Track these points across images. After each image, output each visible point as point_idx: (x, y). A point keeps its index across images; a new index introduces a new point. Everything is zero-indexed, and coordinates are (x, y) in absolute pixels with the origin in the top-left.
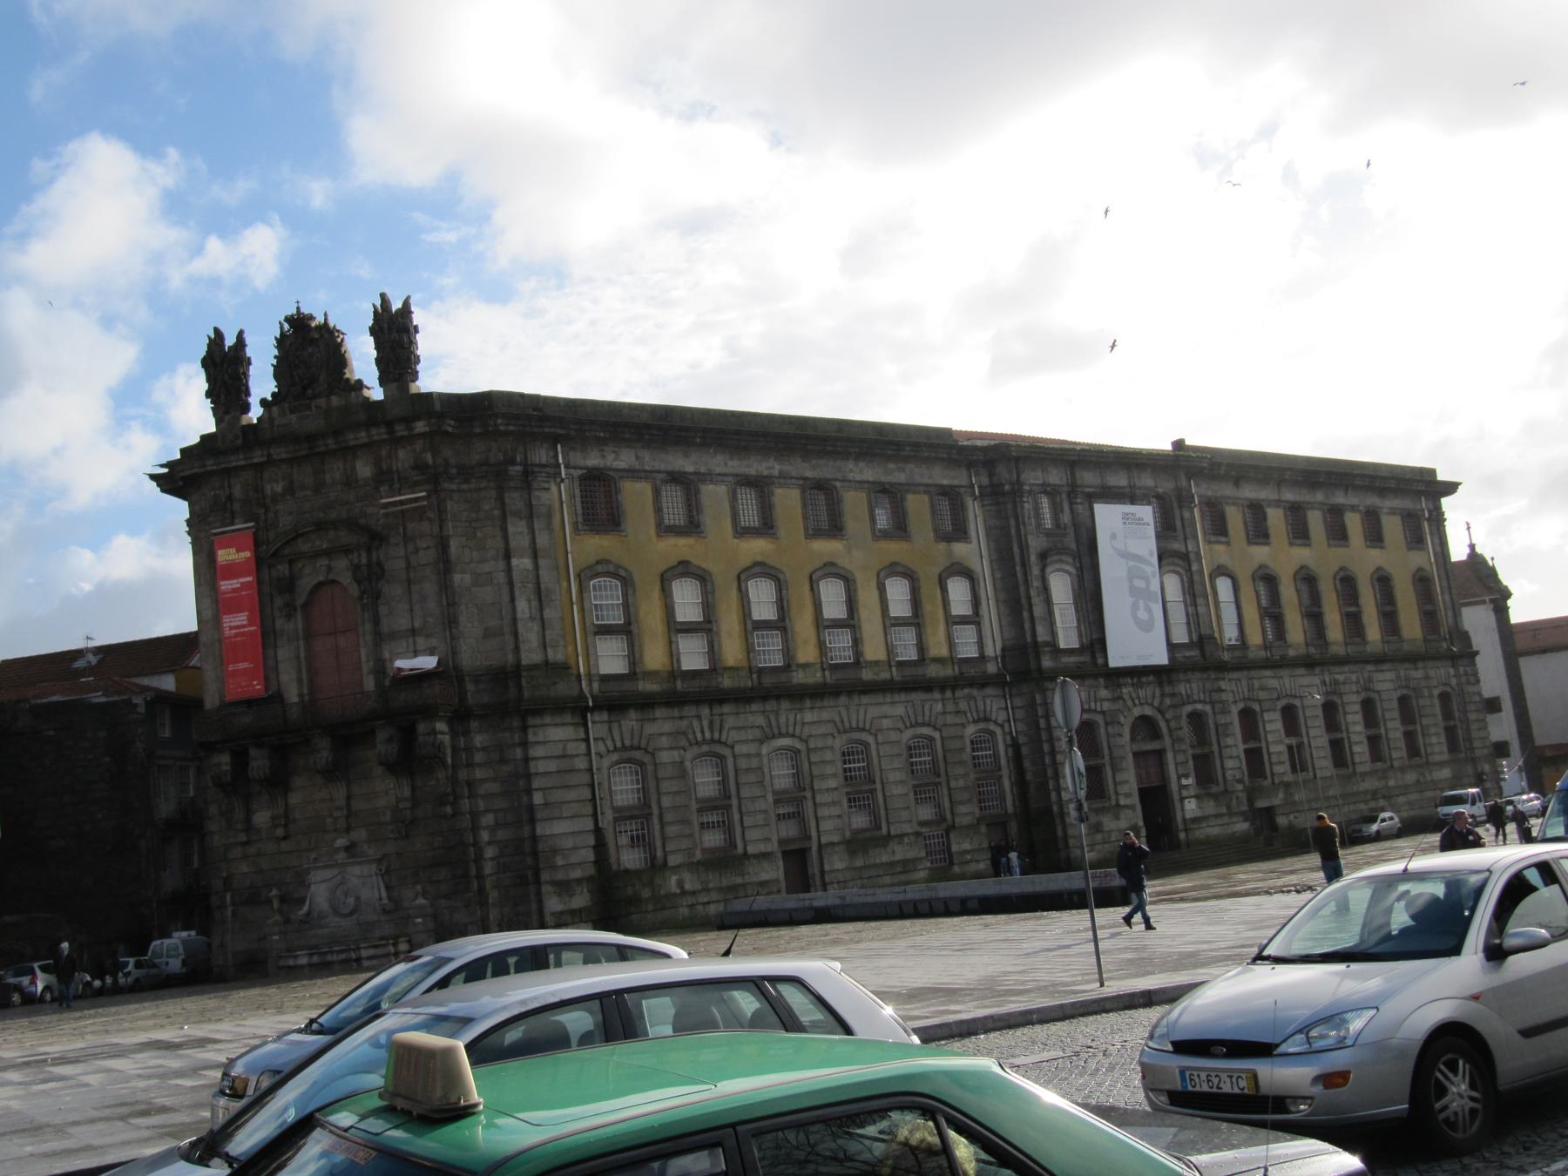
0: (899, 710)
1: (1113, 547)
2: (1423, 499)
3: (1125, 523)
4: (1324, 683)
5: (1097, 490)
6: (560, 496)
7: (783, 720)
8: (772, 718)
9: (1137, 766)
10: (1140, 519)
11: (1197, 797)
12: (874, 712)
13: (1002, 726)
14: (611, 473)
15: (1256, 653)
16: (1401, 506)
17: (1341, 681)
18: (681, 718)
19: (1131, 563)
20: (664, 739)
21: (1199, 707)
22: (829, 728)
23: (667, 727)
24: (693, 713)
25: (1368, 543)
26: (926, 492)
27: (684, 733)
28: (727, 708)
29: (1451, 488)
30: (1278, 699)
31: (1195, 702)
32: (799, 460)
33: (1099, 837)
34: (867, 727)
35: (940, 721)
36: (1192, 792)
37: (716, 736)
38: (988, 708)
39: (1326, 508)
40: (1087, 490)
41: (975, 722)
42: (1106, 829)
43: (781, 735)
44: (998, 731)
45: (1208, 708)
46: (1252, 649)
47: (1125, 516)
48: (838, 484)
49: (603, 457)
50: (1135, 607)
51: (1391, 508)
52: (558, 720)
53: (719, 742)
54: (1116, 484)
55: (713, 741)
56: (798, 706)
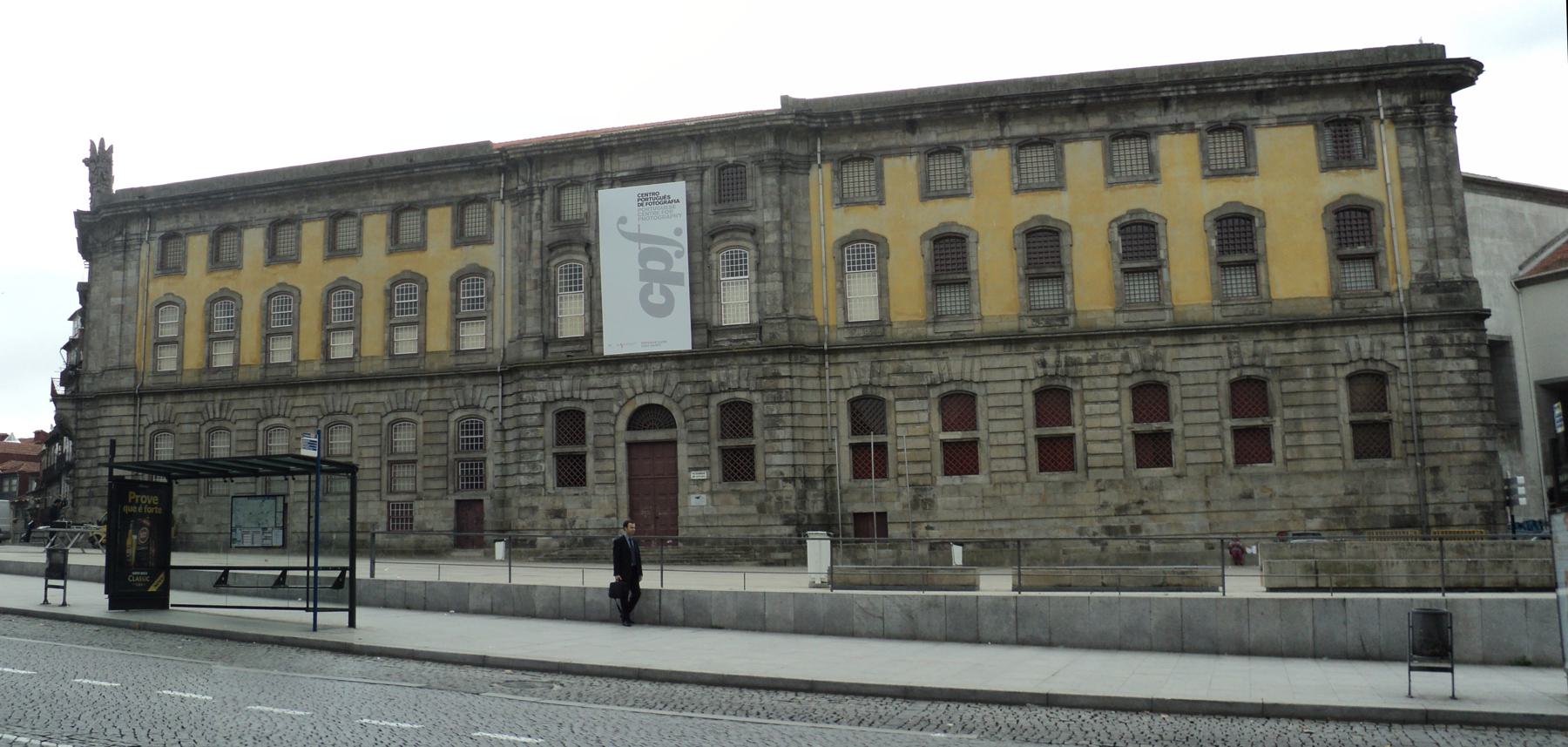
0: (383, 397)
1: (623, 234)
2: (1379, 94)
3: (642, 205)
4: (1044, 364)
5: (635, 173)
6: (148, 253)
7: (276, 403)
8: (269, 402)
9: (630, 458)
10: (664, 197)
11: (711, 493)
12: (355, 399)
13: (491, 411)
14: (181, 232)
15: (899, 332)
16: (1320, 109)
17: (1085, 361)
18: (201, 401)
19: (644, 246)
20: (187, 416)
21: (742, 395)
22: (316, 411)
23: (191, 408)
24: (210, 398)
25: (1207, 172)
26: (447, 204)
27: (201, 413)
28: (235, 395)
29: (1466, 72)
30: (932, 385)
31: (730, 390)
32: (327, 197)
33: (558, 522)
34: (350, 411)
35: (423, 406)
36: (707, 486)
37: (224, 415)
38: (478, 396)
39: (1107, 135)
40: (619, 175)
41: (460, 408)
42: (569, 516)
43: (278, 416)
44: (489, 417)
45: (756, 398)
46: (895, 326)
47: (643, 200)
48: (359, 211)
49: (178, 221)
50: (645, 293)
51: (1279, 117)
52: (119, 402)
53: (225, 419)
54: (665, 161)
55: (220, 419)
56: (292, 394)
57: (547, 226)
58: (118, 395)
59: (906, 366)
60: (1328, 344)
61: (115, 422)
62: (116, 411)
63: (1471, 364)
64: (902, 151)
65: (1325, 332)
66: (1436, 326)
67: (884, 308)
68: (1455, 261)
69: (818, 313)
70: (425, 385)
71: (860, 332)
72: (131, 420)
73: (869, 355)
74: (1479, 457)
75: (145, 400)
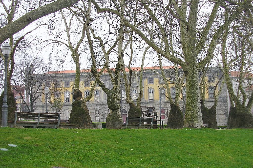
15: (156, 101)
57: (109, 85)
58: (40, 106)
59: (156, 105)
60: (208, 104)
61: (39, 110)
62: (39, 109)
63: (224, 107)
64: (157, 78)
65: (207, 103)
66: (220, 102)
67: (154, 98)
68: (223, 94)
69: (145, 98)
70: (90, 106)
71: (151, 101)
72: (42, 110)
73: (152, 104)
74: (225, 118)
75: (44, 107)
